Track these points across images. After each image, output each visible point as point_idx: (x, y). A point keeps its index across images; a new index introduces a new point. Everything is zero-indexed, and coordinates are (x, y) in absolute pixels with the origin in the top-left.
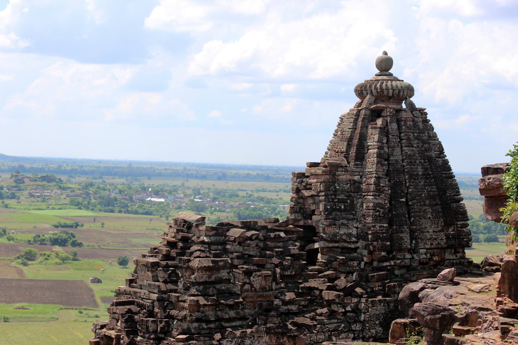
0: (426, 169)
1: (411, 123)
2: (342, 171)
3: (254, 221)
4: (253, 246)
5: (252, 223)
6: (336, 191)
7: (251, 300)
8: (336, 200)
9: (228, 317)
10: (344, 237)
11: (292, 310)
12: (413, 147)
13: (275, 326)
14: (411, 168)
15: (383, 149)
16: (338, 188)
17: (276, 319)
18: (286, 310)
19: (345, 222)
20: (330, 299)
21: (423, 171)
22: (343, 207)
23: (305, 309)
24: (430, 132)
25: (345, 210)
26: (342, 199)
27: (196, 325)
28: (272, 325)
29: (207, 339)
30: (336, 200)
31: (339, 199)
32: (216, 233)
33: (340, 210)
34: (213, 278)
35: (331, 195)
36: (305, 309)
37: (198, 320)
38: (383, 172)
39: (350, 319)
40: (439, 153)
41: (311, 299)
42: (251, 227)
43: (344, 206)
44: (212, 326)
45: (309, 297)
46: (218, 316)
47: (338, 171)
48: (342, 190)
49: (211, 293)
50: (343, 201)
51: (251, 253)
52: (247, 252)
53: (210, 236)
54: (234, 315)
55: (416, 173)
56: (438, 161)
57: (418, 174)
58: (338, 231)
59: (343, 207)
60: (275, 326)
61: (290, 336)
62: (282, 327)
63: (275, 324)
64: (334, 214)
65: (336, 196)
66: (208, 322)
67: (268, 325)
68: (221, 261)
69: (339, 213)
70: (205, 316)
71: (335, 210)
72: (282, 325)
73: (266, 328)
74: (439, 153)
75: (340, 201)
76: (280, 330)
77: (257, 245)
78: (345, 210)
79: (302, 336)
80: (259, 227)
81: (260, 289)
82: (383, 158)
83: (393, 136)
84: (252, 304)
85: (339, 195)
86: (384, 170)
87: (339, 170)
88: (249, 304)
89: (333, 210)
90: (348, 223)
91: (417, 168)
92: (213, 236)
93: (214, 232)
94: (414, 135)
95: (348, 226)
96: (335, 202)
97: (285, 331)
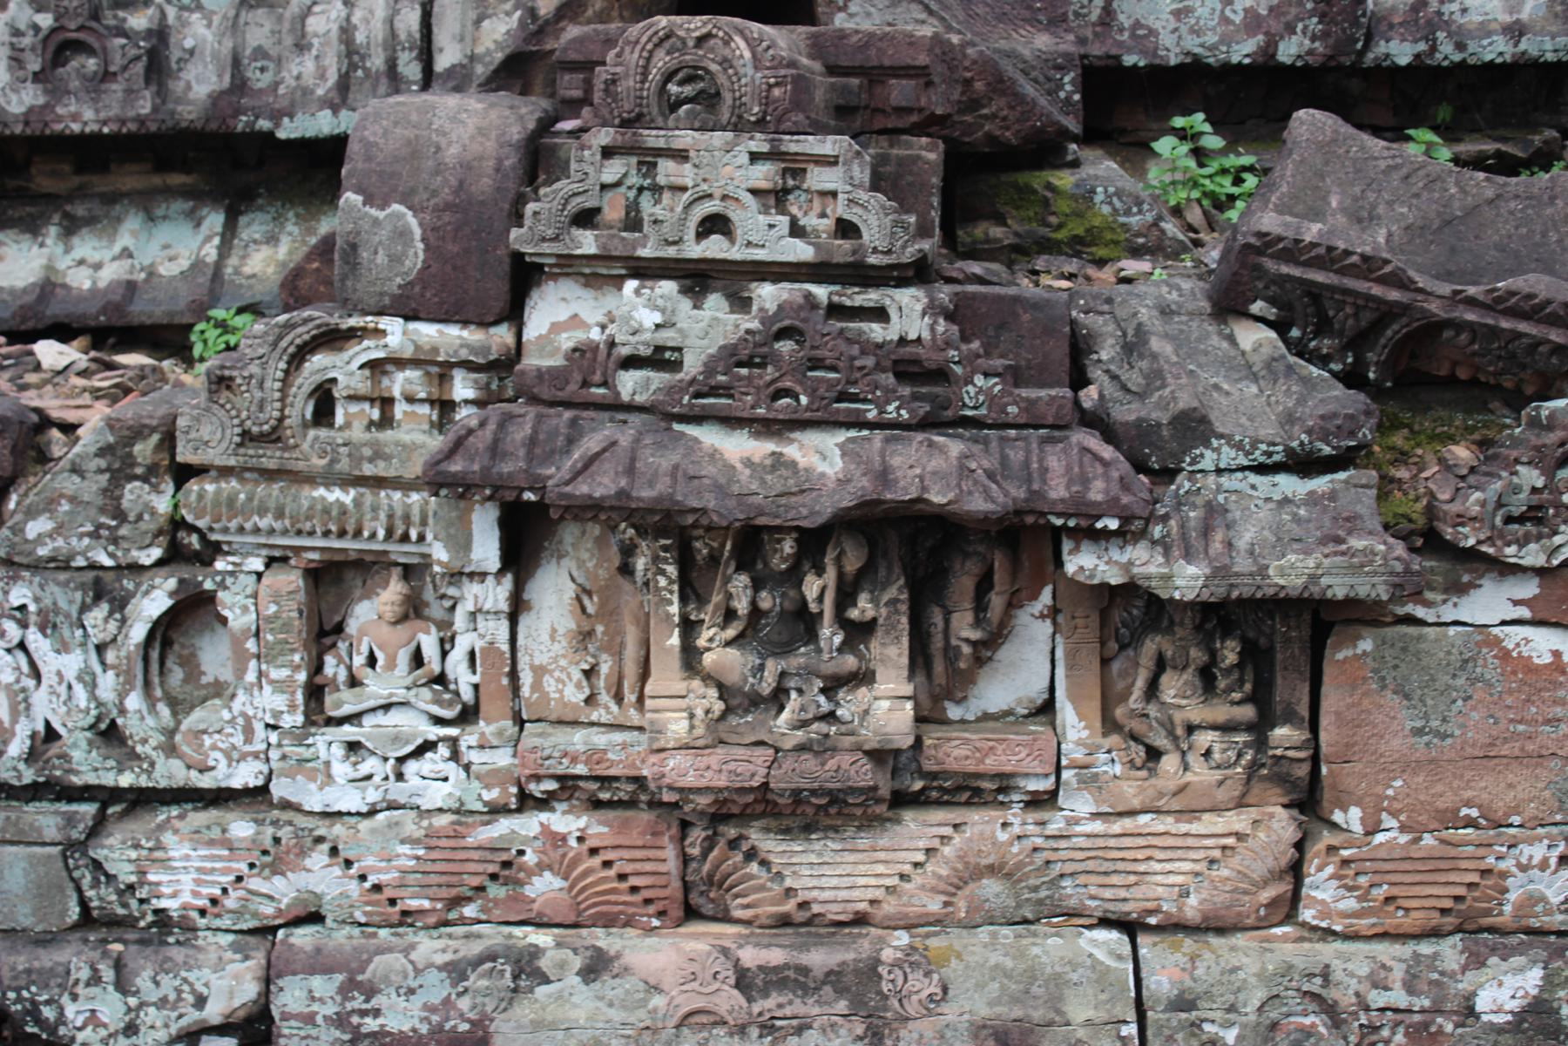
13: (707, 327)
17: (727, 166)
28: (641, 310)
60: (707, 327)
61: (1126, 615)
62: (911, 367)
67: (559, 318)
72: (909, 314)
76: (822, 456)
79: (1489, 604)
97: (932, 471)
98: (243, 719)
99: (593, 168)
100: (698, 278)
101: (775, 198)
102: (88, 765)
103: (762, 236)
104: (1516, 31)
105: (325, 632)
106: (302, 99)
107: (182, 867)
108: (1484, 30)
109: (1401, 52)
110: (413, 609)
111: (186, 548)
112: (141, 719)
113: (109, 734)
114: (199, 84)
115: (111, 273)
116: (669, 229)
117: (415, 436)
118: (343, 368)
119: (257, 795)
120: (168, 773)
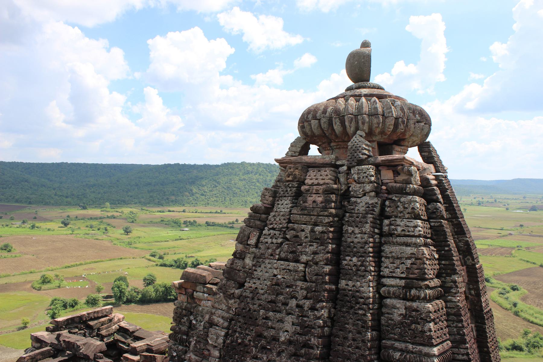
0: (305, 328)
1: (320, 199)
2: (204, 292)
12: (297, 261)
14: (267, 318)
15: (243, 259)
21: (295, 333)
24: (398, 222)
38: (228, 312)
40: (402, 283)
47: (197, 292)
55: (272, 332)
56: (394, 307)
57: (275, 339)
74: (402, 283)
82: (235, 281)
83: (273, 229)
86: (229, 308)
87: (198, 289)
91: (281, 321)
94: (312, 231)
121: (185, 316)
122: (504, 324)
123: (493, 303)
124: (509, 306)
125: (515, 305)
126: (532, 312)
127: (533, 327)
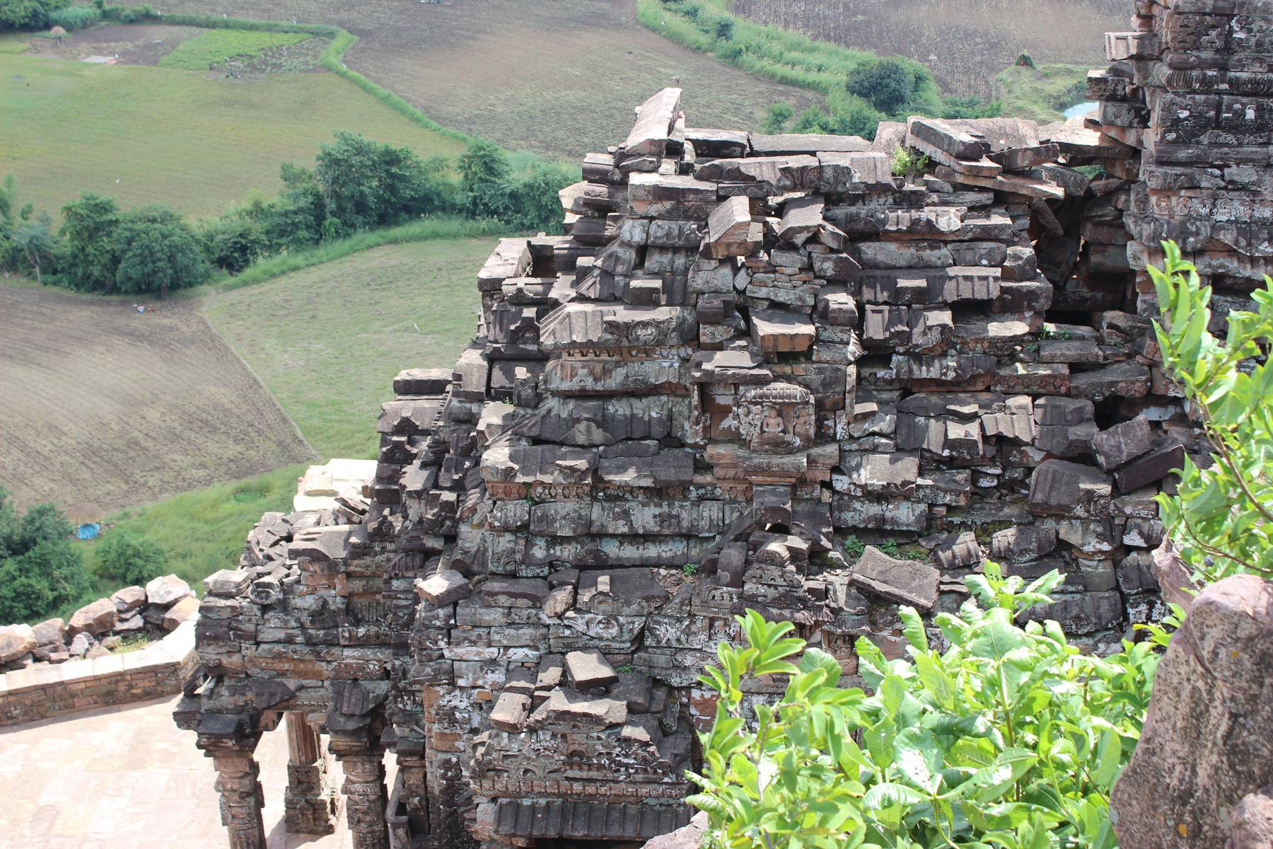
3: (836, 168)
4: (788, 271)
5: (829, 174)
6: (1228, 47)
7: (731, 473)
8: (1225, 86)
9: (626, 530)
10: (1227, 238)
11: (893, 521)
13: (772, 593)
16: (1242, 35)
18: (870, 519)
19: (1245, 174)
20: (1053, 502)
22: (1250, 114)
23: (957, 520)
25: (1259, 127)
26: (1250, 81)
27: (505, 542)
29: (521, 602)
30: (1225, 86)
31: (1234, 83)
32: (675, 209)
33: (1238, 126)
34: (615, 380)
35: (1202, 65)
36: (957, 520)
37: (522, 529)
39: (1127, 579)
41: (1002, 475)
42: (824, 188)
43: (1260, 110)
44: (566, 552)
45: (998, 471)
46: (591, 523)
48: (1259, 44)
49: (581, 439)
50: (1255, 90)
51: (782, 297)
52: (762, 293)
53: (652, 219)
54: (653, 527)
58: (1205, 211)
59: (1250, 114)
60: (772, 593)
63: (776, 587)
64: (1205, 139)
65: (1224, 68)
66: (554, 540)
68: (645, 325)
69: (1230, 138)
70: (544, 518)
71: (1217, 124)
73: (740, 596)
75: (1237, 88)
77: (809, 267)
78: (1259, 127)
80: (855, 187)
81: (761, 444)
84: (741, 487)
85: (1242, 68)
88: (727, 485)
89: (1202, 123)
90: (1259, 183)
92: (661, 217)
93: (668, 205)
95: (1256, 193)
96: (1219, 93)
98: (699, 640)
99: (754, 570)
100: (769, 586)
101: (782, 576)
102: (675, 644)
103: (780, 581)
104: (908, 525)
105: (711, 626)
106: (703, 530)
107: (689, 660)
108: (903, 524)
109: (889, 528)
110: (725, 625)
111: (692, 616)
112: (683, 638)
113: (678, 640)
114: (685, 524)
115: (669, 554)
116: (766, 579)
117: (727, 602)
118: (717, 593)
119: (700, 650)
120: (687, 646)
121: (1214, 27)
122: (702, 101)
123: (653, 36)
124: (704, 40)
125: (724, 30)
126: (776, 47)
127: (786, 95)
